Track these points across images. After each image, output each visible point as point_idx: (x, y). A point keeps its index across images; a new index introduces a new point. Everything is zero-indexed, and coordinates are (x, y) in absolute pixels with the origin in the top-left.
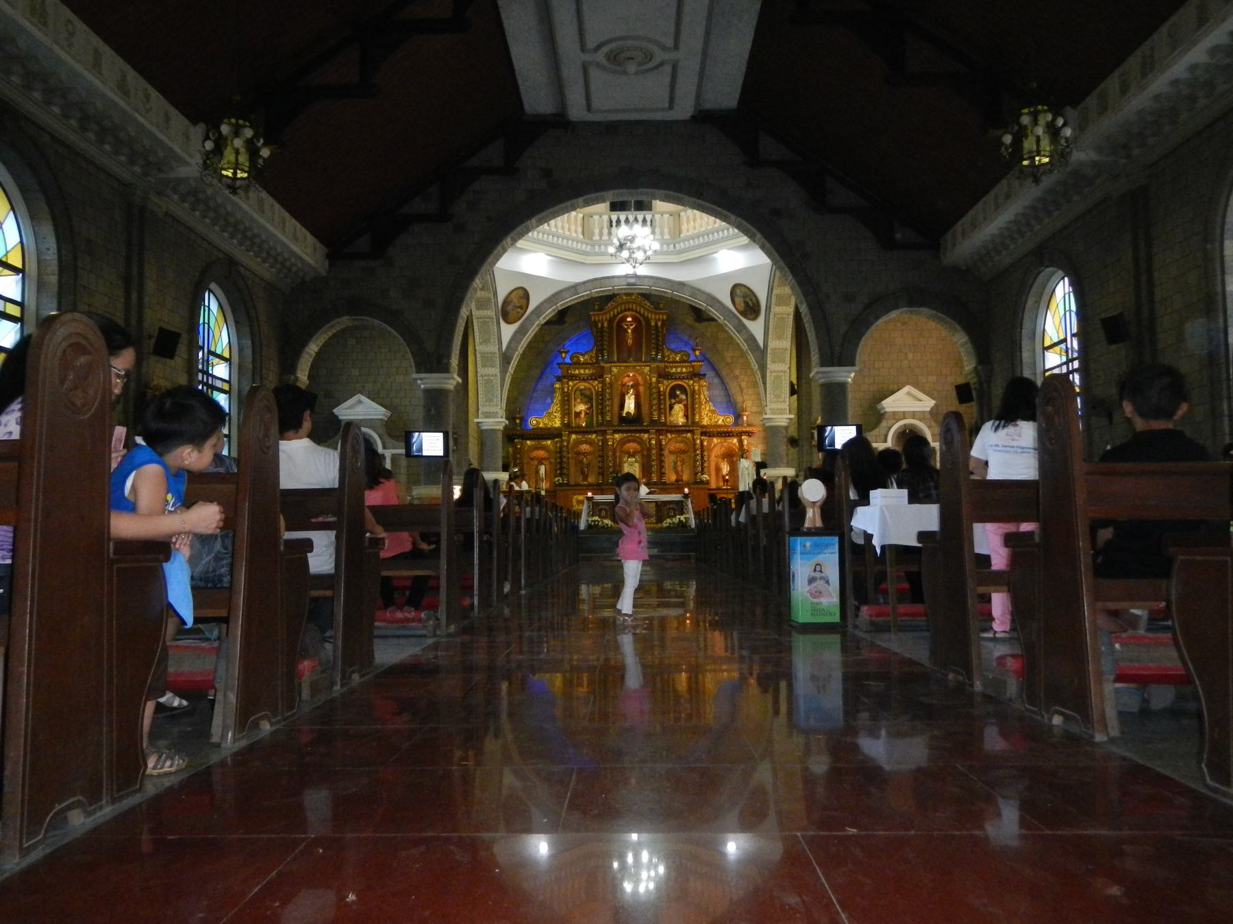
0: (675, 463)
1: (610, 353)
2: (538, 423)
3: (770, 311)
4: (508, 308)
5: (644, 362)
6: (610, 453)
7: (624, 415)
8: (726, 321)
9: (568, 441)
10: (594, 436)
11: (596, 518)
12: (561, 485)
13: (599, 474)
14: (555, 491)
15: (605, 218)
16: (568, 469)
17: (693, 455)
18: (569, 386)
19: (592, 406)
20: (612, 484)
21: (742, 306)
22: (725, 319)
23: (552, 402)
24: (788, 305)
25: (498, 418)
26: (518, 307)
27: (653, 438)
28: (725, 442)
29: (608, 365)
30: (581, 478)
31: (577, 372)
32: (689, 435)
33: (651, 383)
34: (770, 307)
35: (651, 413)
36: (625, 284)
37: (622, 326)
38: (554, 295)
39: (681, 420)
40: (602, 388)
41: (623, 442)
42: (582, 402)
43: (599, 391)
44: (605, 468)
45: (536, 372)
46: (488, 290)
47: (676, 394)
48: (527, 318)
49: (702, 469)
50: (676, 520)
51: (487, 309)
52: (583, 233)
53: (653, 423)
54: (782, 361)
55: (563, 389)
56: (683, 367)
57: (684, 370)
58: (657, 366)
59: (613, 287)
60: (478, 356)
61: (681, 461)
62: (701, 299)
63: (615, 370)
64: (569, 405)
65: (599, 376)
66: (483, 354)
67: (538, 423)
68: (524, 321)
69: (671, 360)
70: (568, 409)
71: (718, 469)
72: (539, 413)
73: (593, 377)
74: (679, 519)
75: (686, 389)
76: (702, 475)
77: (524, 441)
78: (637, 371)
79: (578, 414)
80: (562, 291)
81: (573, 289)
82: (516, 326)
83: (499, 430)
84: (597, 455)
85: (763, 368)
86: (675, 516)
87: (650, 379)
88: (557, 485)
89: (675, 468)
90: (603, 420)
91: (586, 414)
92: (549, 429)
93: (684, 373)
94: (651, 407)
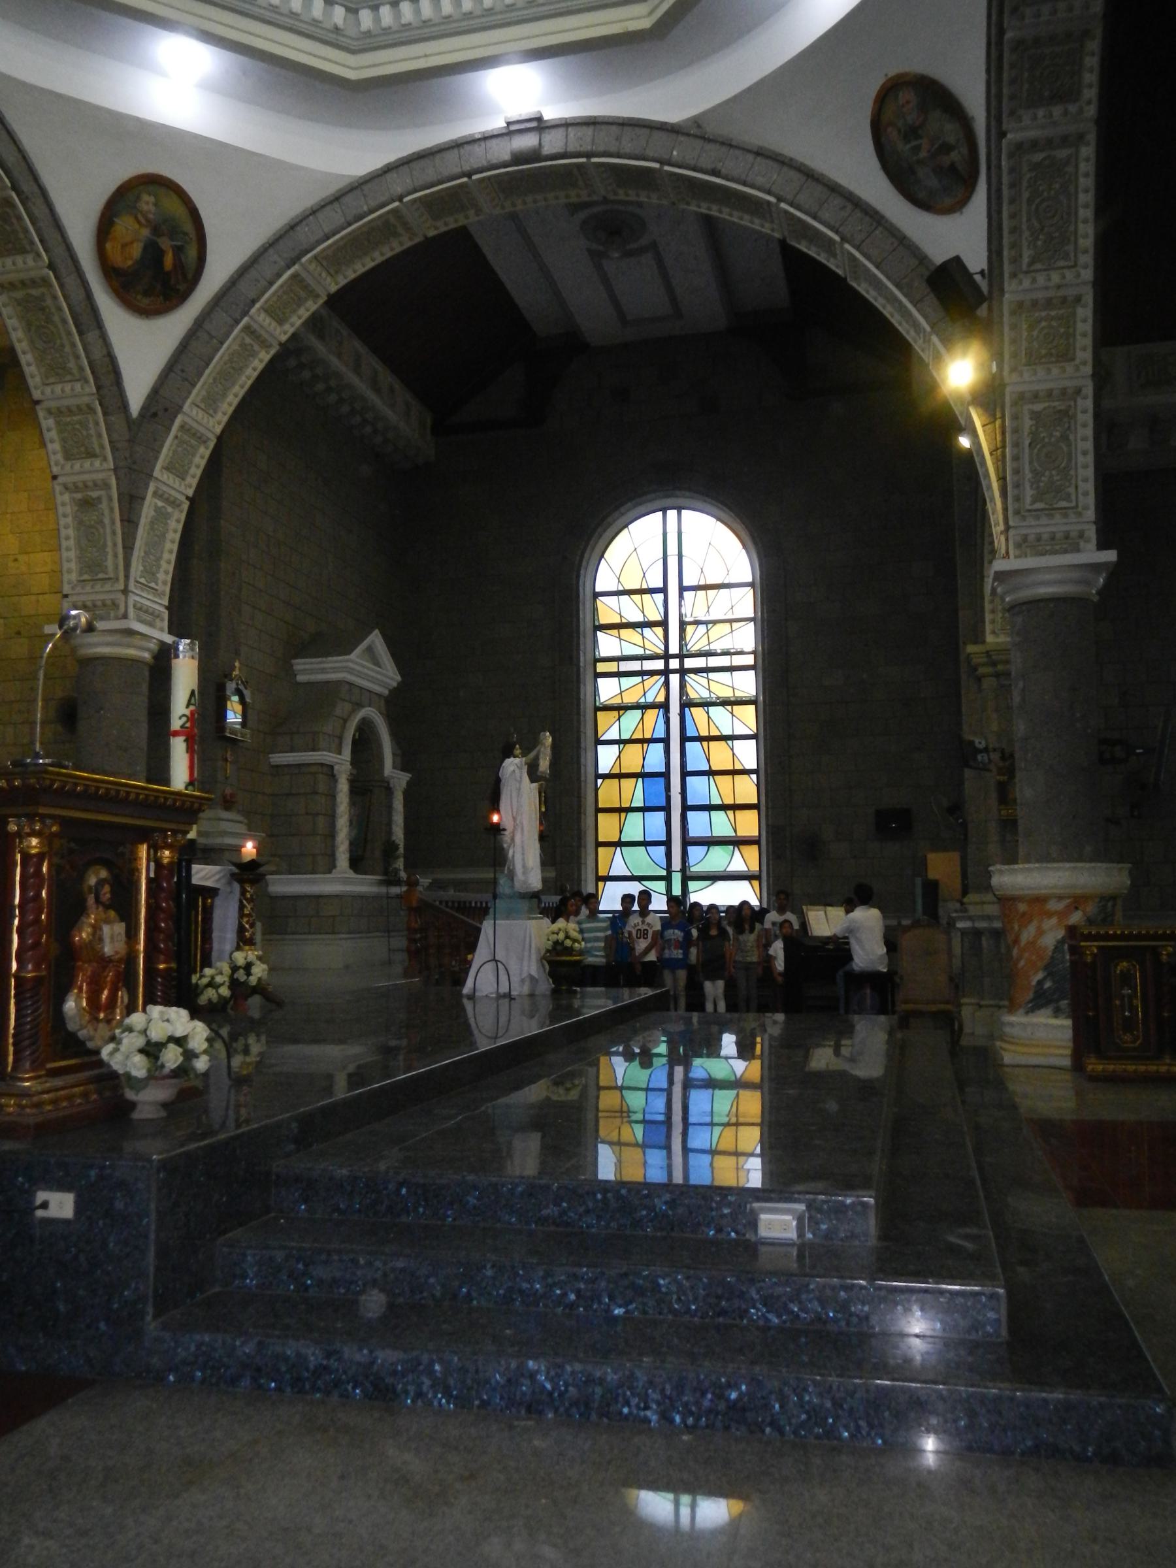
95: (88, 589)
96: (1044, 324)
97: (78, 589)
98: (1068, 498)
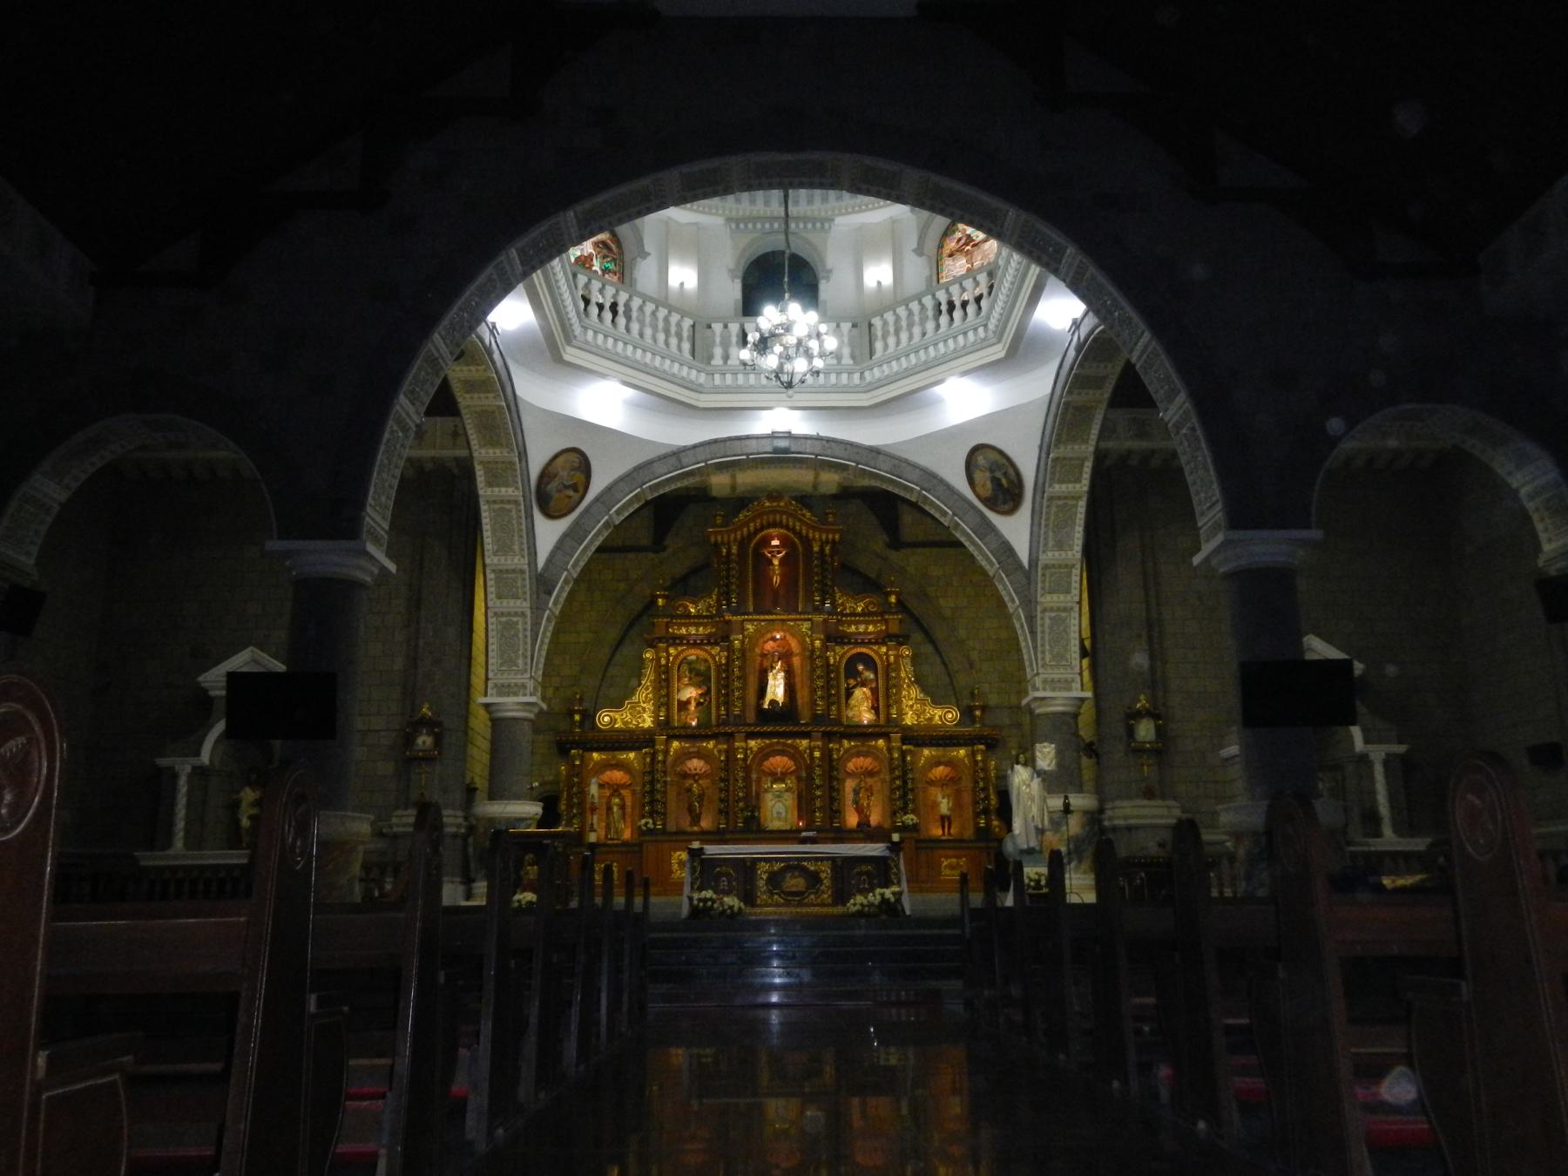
0: (856, 792)
1: (742, 600)
2: (613, 721)
3: (1044, 492)
4: (549, 487)
5: (801, 614)
6: (741, 774)
7: (766, 706)
8: (956, 518)
9: (666, 752)
10: (711, 744)
11: (709, 894)
12: (651, 832)
13: (720, 812)
14: (640, 845)
15: (734, 328)
16: (664, 804)
17: (888, 778)
18: (669, 655)
19: (708, 692)
20: (742, 831)
21: (987, 489)
22: (954, 514)
23: (640, 684)
24: (1078, 480)
25: (525, 695)
26: (566, 487)
27: (818, 747)
29: (739, 618)
30: (688, 823)
31: (683, 631)
32: (881, 742)
33: (813, 651)
34: (1044, 483)
35: (814, 703)
36: (769, 449)
37: (764, 554)
38: (638, 468)
39: (867, 717)
40: (728, 658)
41: (764, 754)
42: (690, 685)
43: (721, 665)
44: (731, 803)
45: (613, 634)
46: (509, 445)
47: (858, 671)
48: (587, 510)
49: (906, 804)
50: (874, 897)
51: (507, 485)
52: (693, 353)
53: (817, 719)
54: (1068, 591)
55: (658, 659)
56: (867, 623)
57: (871, 628)
58: (824, 620)
59: (748, 455)
60: (491, 576)
61: (867, 790)
62: (909, 478)
63: (750, 627)
64: (668, 687)
65: (721, 637)
66: (499, 572)
67: (613, 721)
68: (581, 515)
69: (848, 611)
70: (668, 695)
72: (617, 704)
73: (710, 641)
74: (882, 895)
75: (875, 663)
76: (906, 814)
77: (586, 754)
78: (788, 630)
79: (684, 705)
80: (649, 463)
81: (673, 460)
82: (563, 525)
83: (525, 719)
84: (717, 778)
85: (1029, 602)
86: (872, 890)
87: (812, 644)
88: (642, 833)
89: (856, 802)
90: (726, 715)
91: (699, 704)
92: (631, 732)
93: (870, 633)
94: (813, 691)
95: (505, 676)
96: (1057, 575)
97: (499, 676)
98: (1067, 661)
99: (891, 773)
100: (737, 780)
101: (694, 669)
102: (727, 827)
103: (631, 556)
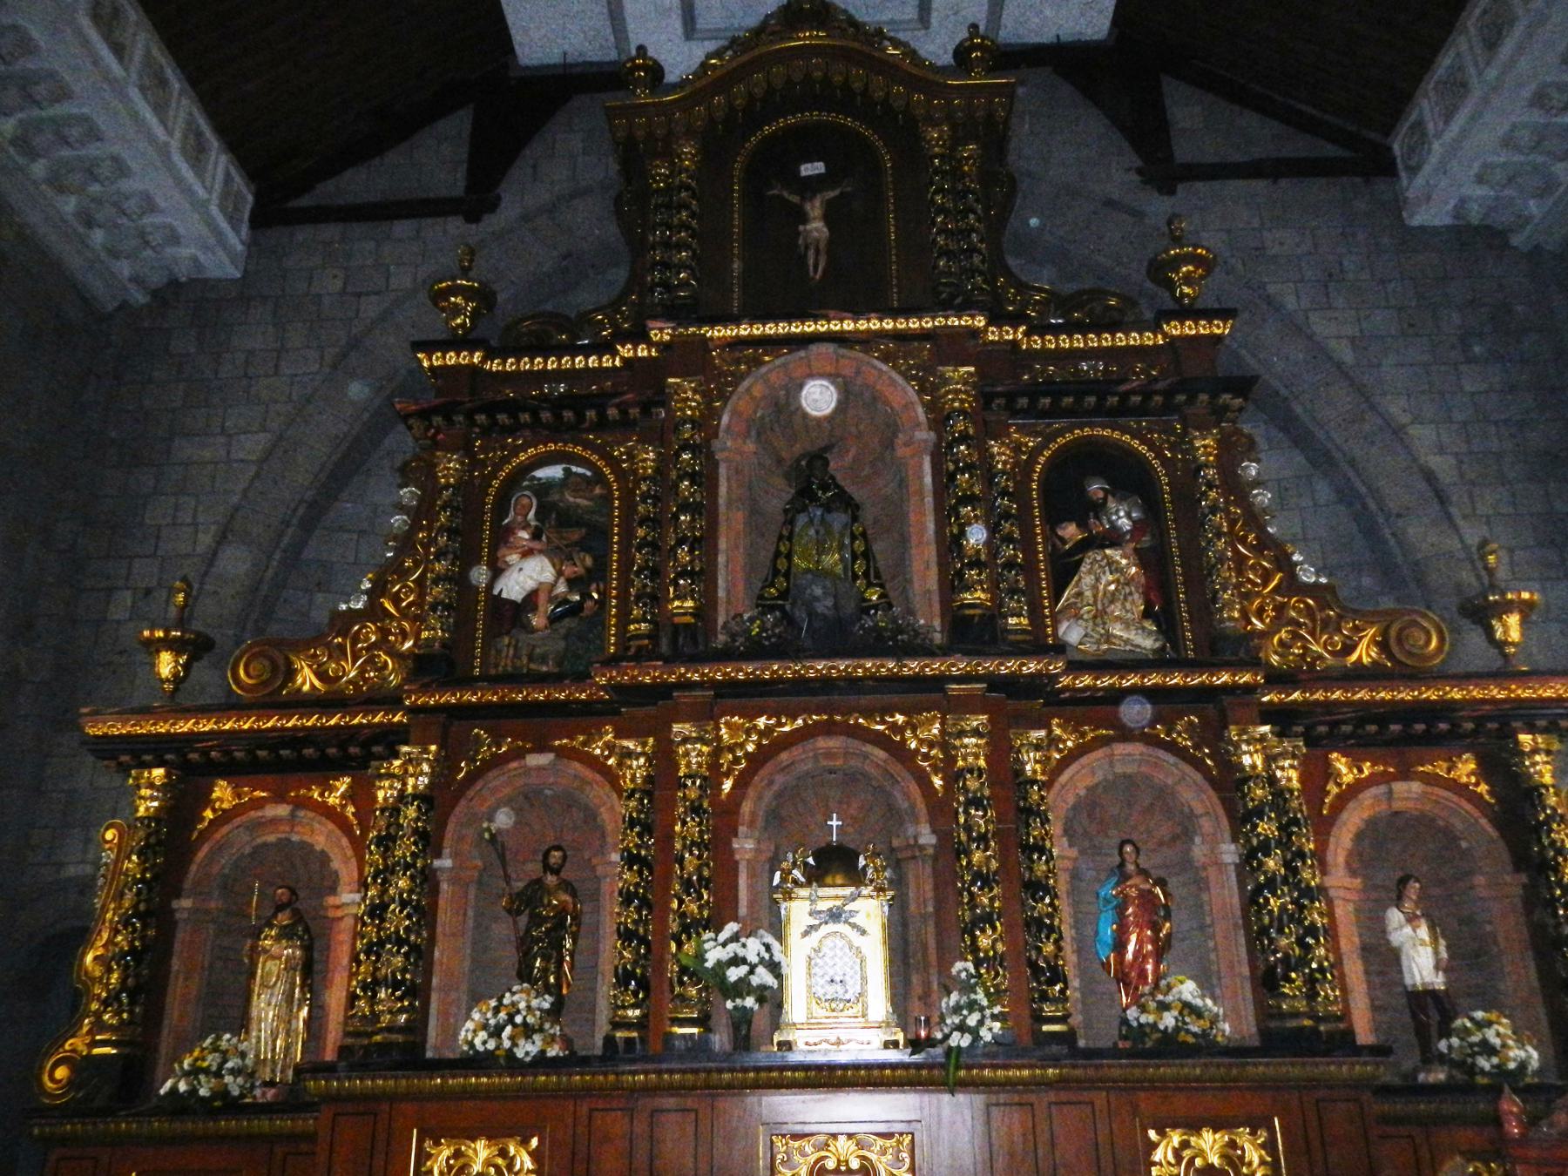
5: (895, 314)
17: (1230, 853)
19: (598, 572)
28: (1405, 774)
71: (1384, 959)
99: (1235, 840)
100: (681, 860)
101: (554, 505)
102: (643, 1040)
103: (402, 228)
